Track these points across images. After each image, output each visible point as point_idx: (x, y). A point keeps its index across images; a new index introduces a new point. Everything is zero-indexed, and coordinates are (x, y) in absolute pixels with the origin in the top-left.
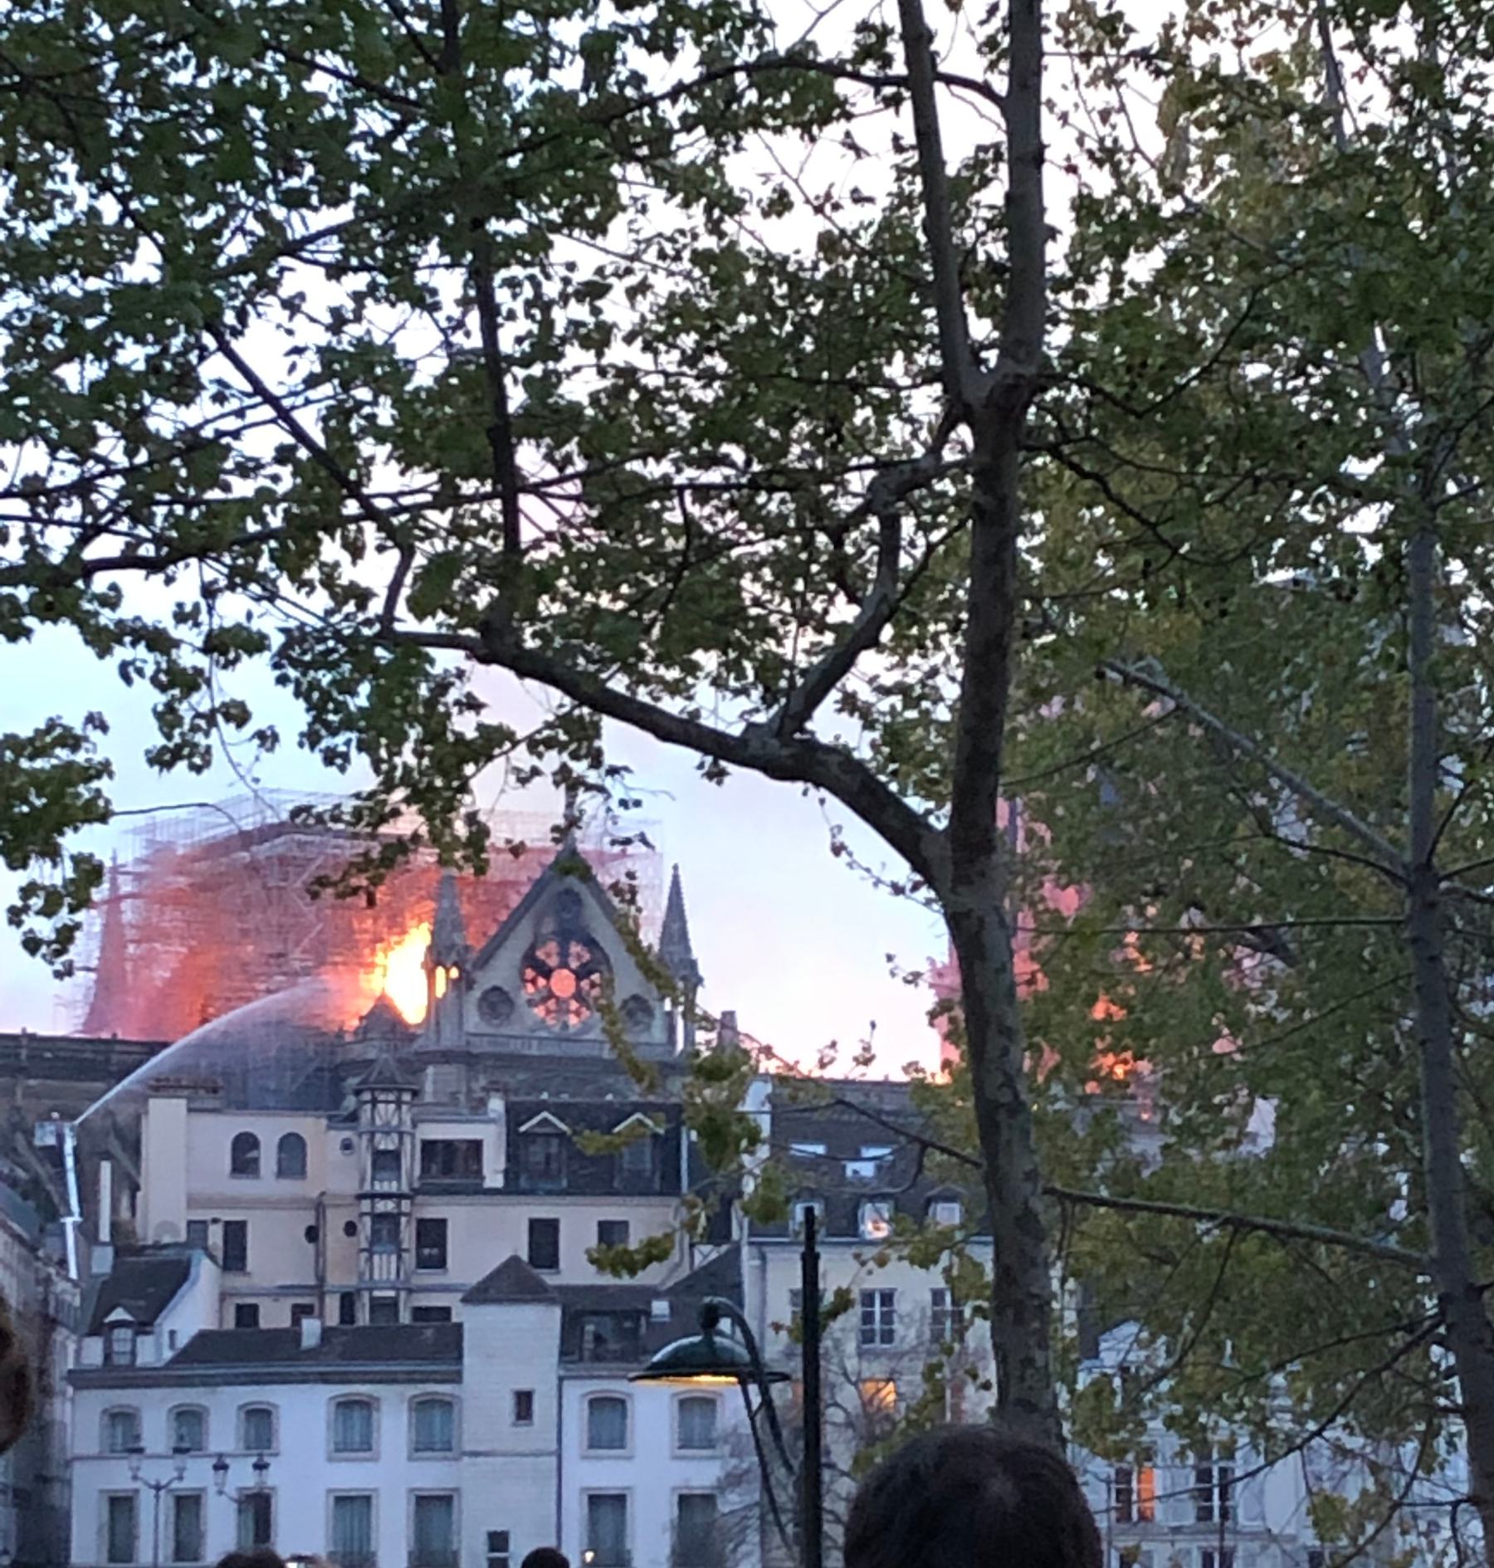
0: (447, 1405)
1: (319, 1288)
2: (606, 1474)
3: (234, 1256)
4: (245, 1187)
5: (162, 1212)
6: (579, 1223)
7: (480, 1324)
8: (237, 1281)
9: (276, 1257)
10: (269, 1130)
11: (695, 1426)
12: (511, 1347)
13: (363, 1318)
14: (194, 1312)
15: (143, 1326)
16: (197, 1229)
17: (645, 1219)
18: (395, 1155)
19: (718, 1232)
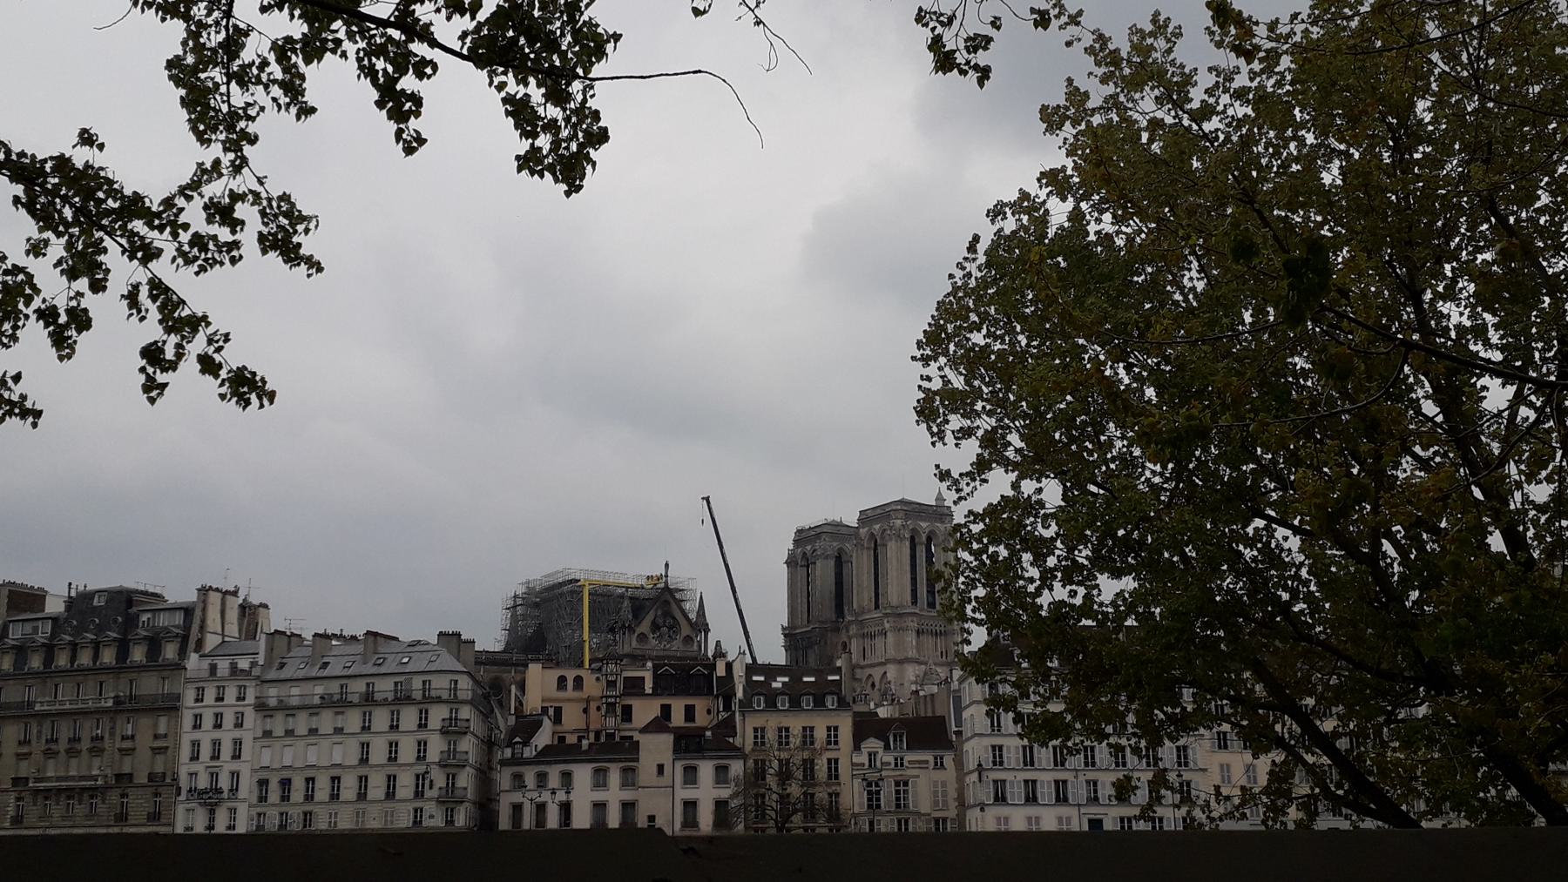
0: (633, 770)
1: (587, 730)
2: (690, 794)
3: (557, 719)
4: (561, 694)
5: (533, 702)
6: (678, 706)
7: (646, 741)
8: (559, 728)
9: (573, 718)
10: (571, 675)
12: (656, 749)
13: (603, 739)
14: (543, 738)
15: (526, 743)
16: (545, 710)
17: (700, 704)
18: (614, 682)
19: (727, 707)
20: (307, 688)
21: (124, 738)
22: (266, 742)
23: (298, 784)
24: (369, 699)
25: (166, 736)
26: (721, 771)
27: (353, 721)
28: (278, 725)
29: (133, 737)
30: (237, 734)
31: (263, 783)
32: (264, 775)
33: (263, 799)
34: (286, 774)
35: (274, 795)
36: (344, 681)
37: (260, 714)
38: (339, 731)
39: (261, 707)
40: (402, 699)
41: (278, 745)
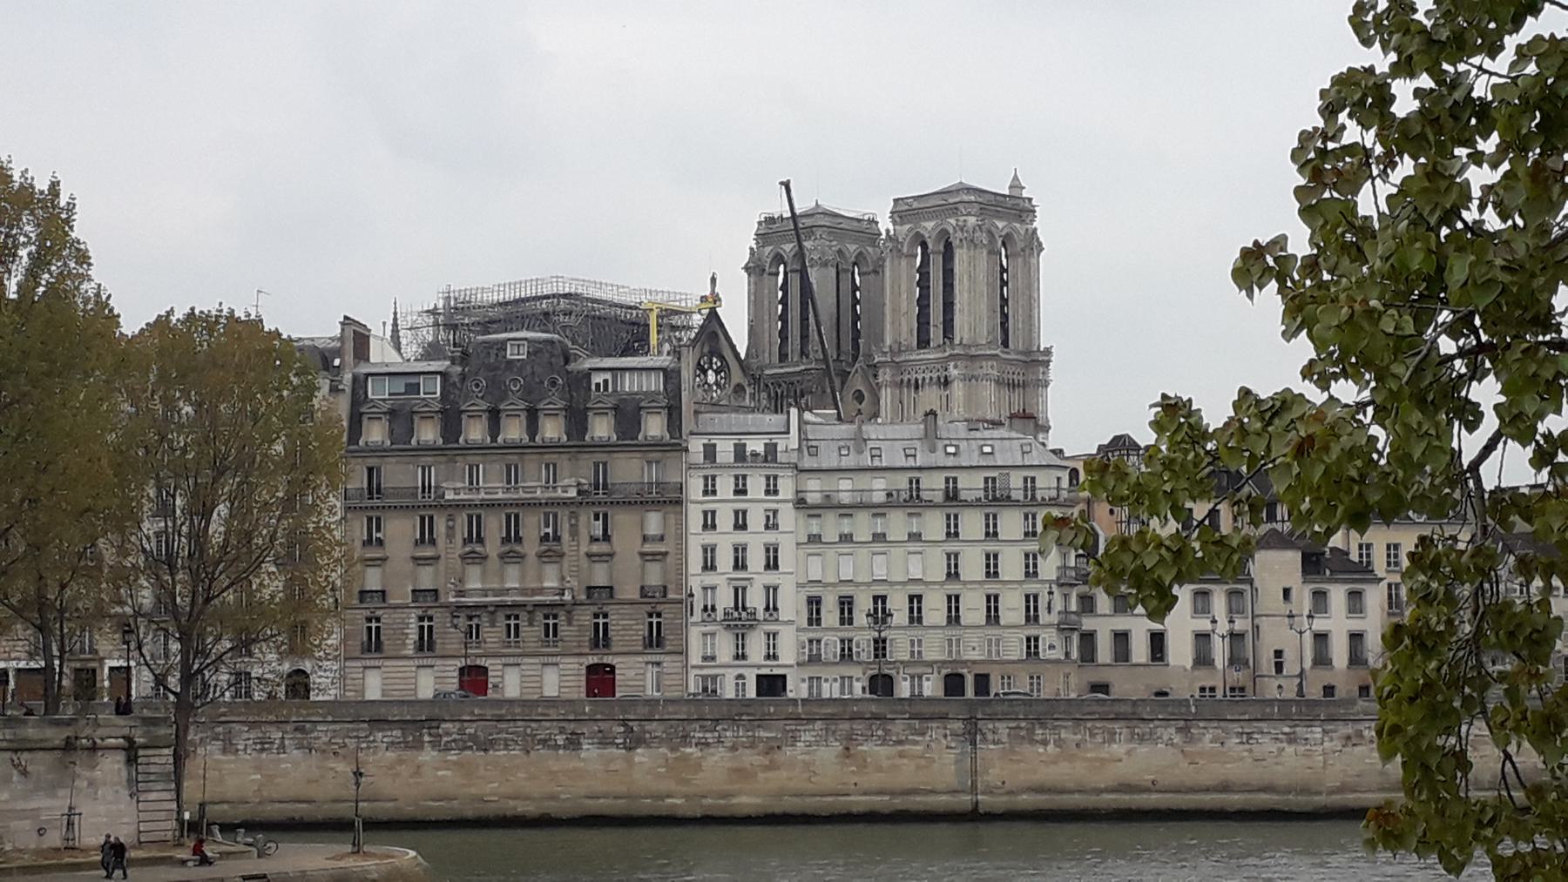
11: (1355, 601)
20: (863, 481)
21: (594, 540)
22: (813, 548)
23: (864, 604)
24: (952, 496)
25: (662, 538)
26: (1355, 598)
27: (933, 526)
28: (831, 527)
29: (606, 537)
30: (771, 537)
31: (814, 603)
32: (815, 591)
33: (814, 619)
34: (846, 590)
35: (830, 616)
36: (916, 474)
37: (802, 514)
38: (915, 537)
39: (800, 503)
40: (995, 498)
41: (831, 553)
